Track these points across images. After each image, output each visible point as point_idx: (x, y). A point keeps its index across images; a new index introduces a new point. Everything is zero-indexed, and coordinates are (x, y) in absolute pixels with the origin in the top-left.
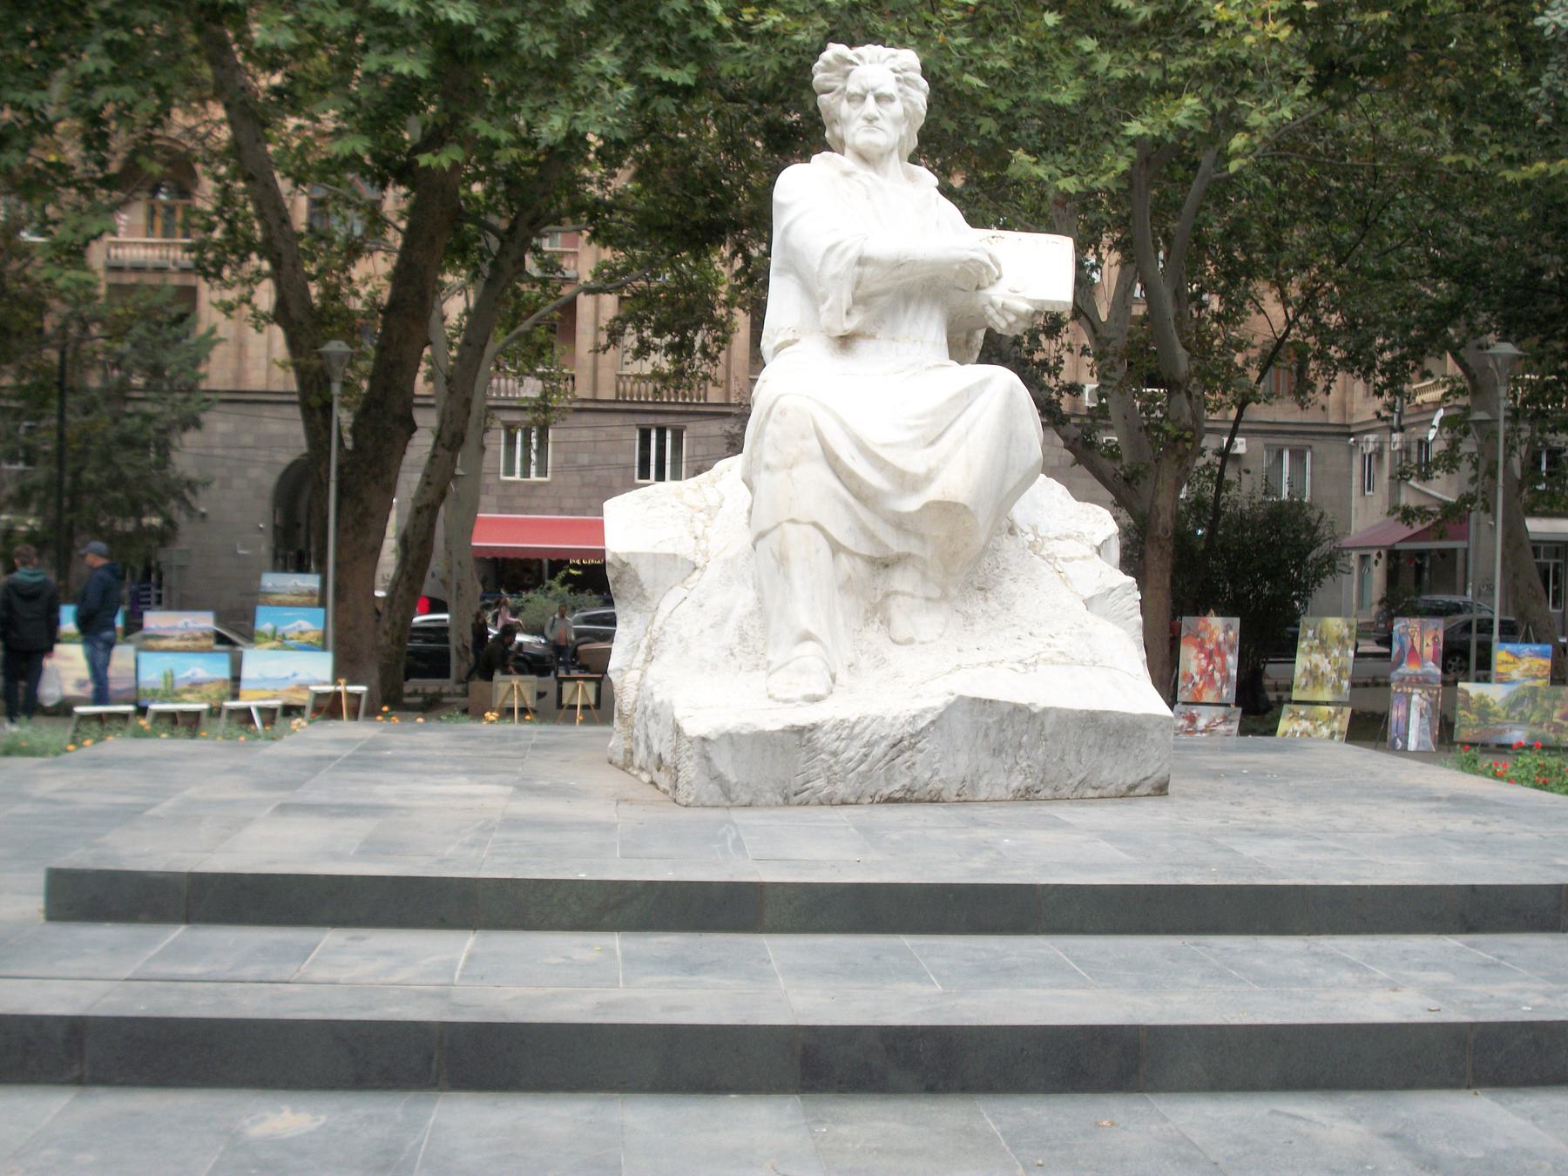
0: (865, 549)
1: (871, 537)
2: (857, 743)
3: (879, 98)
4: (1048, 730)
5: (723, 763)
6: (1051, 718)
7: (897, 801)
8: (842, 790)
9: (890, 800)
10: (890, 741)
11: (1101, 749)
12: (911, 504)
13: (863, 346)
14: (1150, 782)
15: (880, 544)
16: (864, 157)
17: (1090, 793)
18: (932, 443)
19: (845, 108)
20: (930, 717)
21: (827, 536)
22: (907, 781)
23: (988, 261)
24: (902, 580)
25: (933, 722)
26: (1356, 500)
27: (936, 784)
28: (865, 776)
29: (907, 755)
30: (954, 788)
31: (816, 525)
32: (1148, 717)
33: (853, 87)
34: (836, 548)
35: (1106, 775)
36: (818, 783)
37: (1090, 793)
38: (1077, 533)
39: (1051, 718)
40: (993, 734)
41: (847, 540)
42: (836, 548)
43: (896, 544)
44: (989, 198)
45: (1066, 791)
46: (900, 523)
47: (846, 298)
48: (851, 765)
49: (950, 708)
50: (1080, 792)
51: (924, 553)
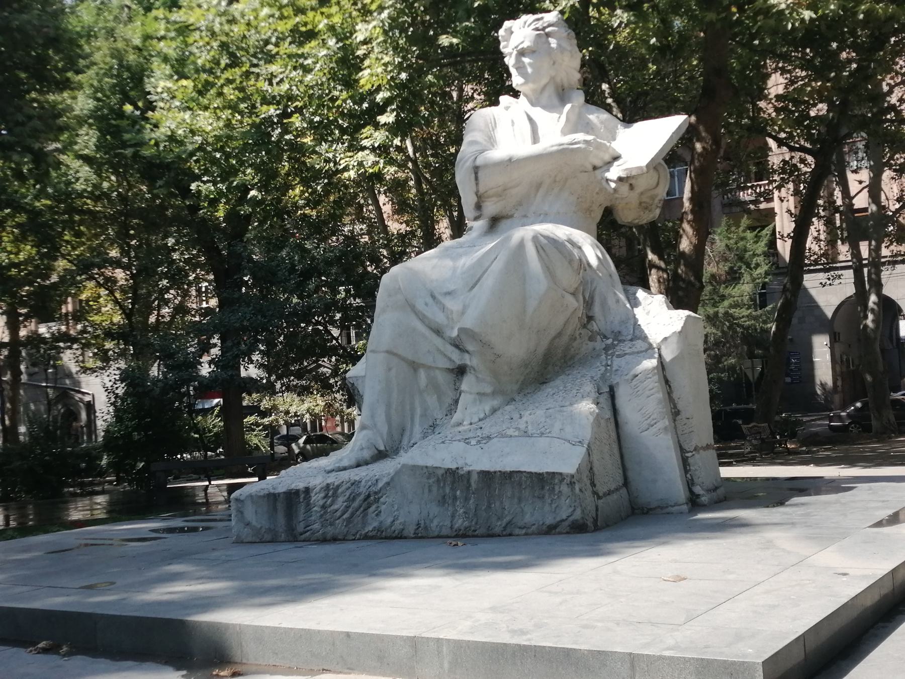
0: (443, 363)
2: (341, 499)
4: (474, 486)
5: (250, 513)
6: (474, 477)
7: (372, 538)
8: (330, 531)
9: (366, 537)
10: (362, 497)
11: (520, 500)
14: (567, 523)
15: (450, 359)
17: (517, 531)
18: (473, 287)
20: (385, 480)
22: (376, 524)
24: (467, 384)
25: (388, 484)
27: (397, 526)
28: (349, 520)
29: (373, 508)
30: (410, 530)
35: (528, 519)
36: (316, 526)
37: (517, 531)
39: (474, 477)
40: (435, 489)
41: (428, 360)
42: (414, 366)
43: (457, 358)
45: (497, 530)
48: (338, 514)
49: (398, 473)
50: (508, 531)
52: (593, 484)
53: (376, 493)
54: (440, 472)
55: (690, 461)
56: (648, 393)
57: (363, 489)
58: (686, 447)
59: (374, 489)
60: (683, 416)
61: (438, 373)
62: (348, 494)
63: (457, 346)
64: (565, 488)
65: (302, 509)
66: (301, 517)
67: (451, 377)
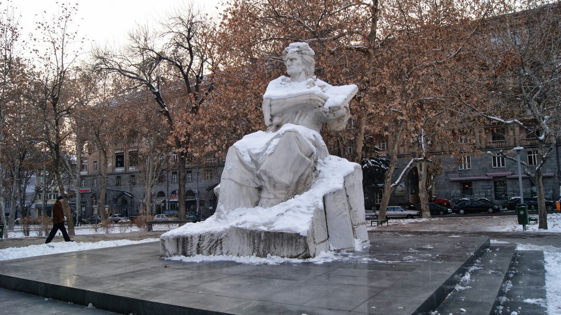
1: (254, 182)
4: (263, 238)
6: (263, 235)
10: (214, 241)
20: (225, 234)
21: (236, 182)
23: (319, 99)
31: (231, 179)
34: (241, 185)
39: (263, 235)
48: (205, 248)
52: (314, 239)
53: (221, 240)
54: (248, 232)
55: (356, 229)
56: (339, 200)
57: (215, 238)
58: (354, 223)
59: (220, 238)
60: (354, 209)
61: (251, 189)
62: (209, 239)
64: (302, 241)
65: (189, 245)
66: (189, 248)
67: (257, 191)
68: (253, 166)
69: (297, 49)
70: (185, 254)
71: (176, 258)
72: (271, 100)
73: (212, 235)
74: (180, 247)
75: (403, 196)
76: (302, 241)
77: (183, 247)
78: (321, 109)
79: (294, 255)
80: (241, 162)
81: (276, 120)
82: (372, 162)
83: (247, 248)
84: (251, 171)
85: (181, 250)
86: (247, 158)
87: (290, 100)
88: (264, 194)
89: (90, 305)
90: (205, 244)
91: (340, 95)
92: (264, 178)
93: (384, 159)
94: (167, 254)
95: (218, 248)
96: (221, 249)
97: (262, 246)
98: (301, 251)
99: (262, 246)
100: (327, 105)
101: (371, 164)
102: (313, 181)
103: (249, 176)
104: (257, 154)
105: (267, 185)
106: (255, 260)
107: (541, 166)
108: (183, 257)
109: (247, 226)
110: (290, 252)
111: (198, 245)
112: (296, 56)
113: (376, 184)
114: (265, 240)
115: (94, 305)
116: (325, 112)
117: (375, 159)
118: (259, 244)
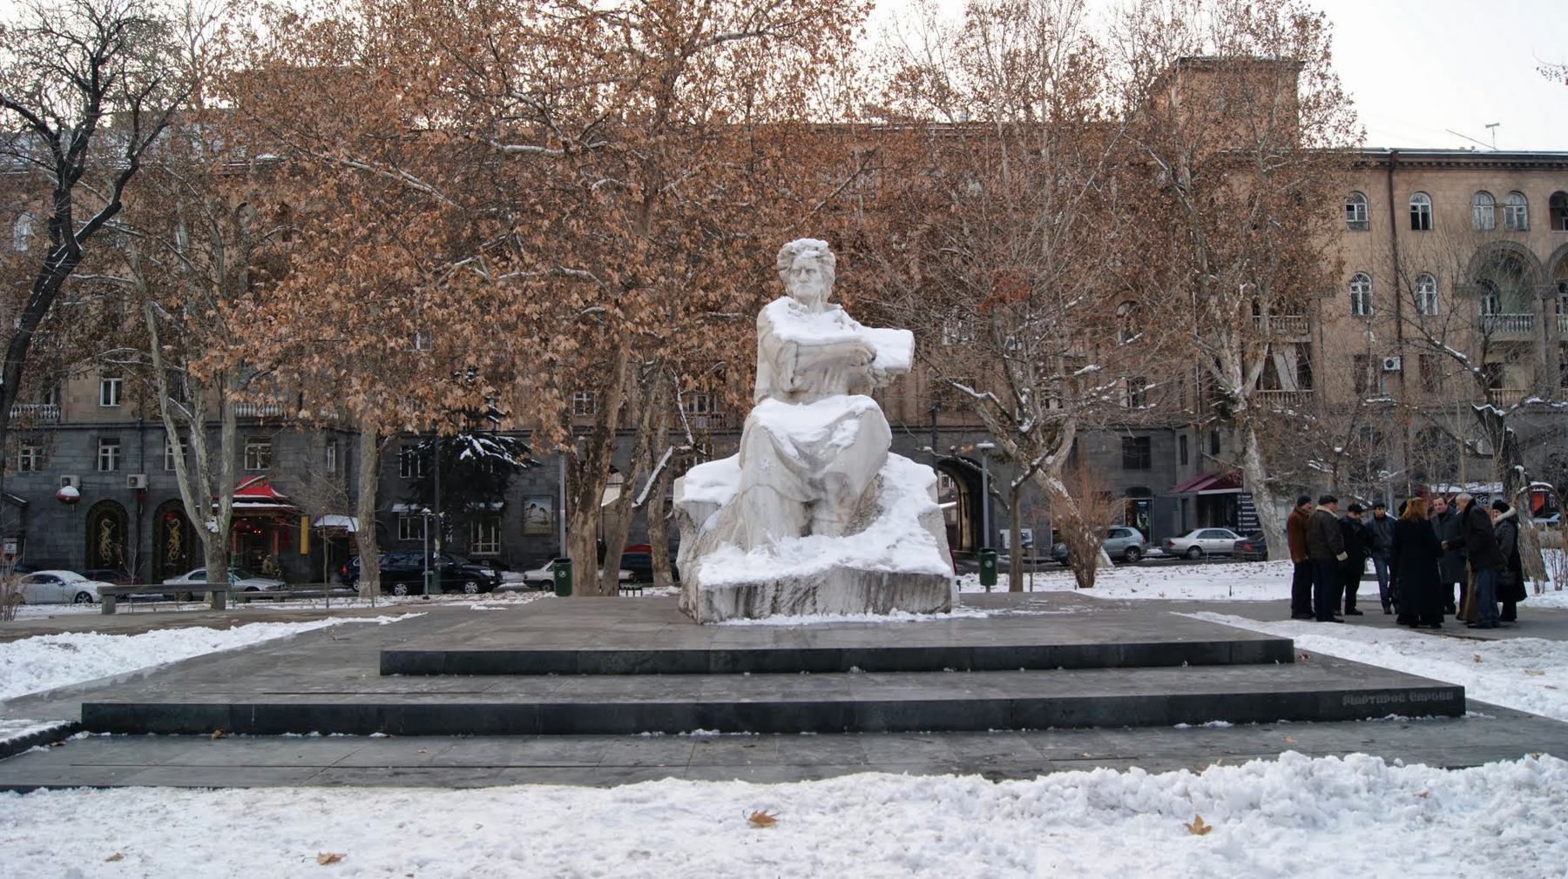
1: (801, 492)
3: (808, 271)
6: (885, 578)
12: (818, 476)
13: (802, 396)
15: (807, 496)
16: (802, 300)
19: (792, 278)
21: (777, 493)
26: (1179, 468)
32: (940, 578)
33: (795, 267)
34: (782, 497)
38: (914, 485)
39: (885, 578)
43: (813, 496)
44: (871, 314)
46: (812, 483)
47: (791, 375)
51: (819, 497)
63: (812, 483)
65: (759, 599)
68: (804, 464)
69: (816, 253)
70: (749, 615)
71: (736, 622)
72: (798, 345)
73: (796, 580)
74: (741, 603)
75: (544, 535)
76: (943, 586)
77: (747, 604)
78: (865, 368)
79: (929, 608)
80: (780, 456)
81: (798, 382)
82: (483, 445)
83: (855, 601)
84: (799, 473)
85: (741, 608)
86: (790, 450)
87: (827, 349)
88: (822, 514)
89: (855, 669)
90: (785, 596)
91: (893, 347)
92: (832, 486)
93: (509, 439)
94: (716, 617)
95: (809, 602)
96: (814, 603)
97: (881, 597)
98: (940, 602)
99: (881, 597)
100: (880, 364)
101: (480, 448)
102: (877, 493)
103: (794, 481)
104: (810, 445)
105: (832, 498)
106: (871, 617)
107: (1026, 478)
108: (747, 621)
109: (856, 564)
110: (923, 606)
111: (775, 598)
112: (815, 265)
113: (487, 502)
114: (888, 587)
115: (861, 667)
116: (875, 376)
117: (492, 440)
118: (877, 592)
